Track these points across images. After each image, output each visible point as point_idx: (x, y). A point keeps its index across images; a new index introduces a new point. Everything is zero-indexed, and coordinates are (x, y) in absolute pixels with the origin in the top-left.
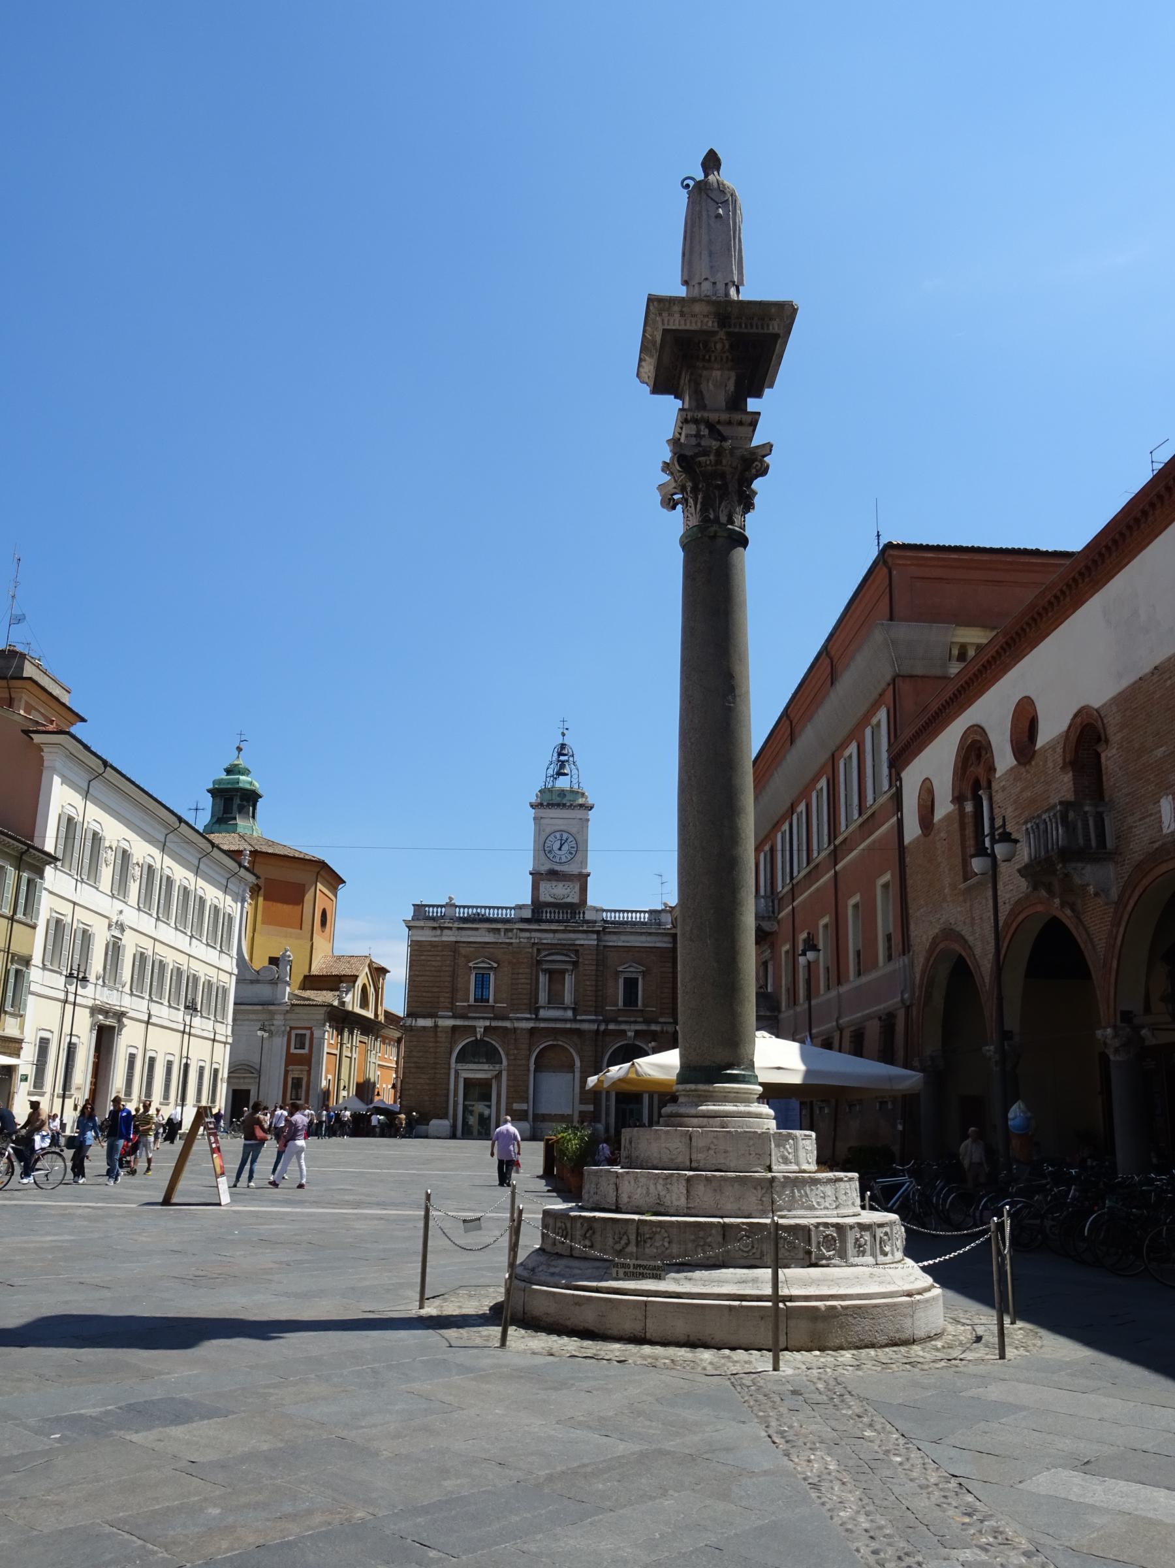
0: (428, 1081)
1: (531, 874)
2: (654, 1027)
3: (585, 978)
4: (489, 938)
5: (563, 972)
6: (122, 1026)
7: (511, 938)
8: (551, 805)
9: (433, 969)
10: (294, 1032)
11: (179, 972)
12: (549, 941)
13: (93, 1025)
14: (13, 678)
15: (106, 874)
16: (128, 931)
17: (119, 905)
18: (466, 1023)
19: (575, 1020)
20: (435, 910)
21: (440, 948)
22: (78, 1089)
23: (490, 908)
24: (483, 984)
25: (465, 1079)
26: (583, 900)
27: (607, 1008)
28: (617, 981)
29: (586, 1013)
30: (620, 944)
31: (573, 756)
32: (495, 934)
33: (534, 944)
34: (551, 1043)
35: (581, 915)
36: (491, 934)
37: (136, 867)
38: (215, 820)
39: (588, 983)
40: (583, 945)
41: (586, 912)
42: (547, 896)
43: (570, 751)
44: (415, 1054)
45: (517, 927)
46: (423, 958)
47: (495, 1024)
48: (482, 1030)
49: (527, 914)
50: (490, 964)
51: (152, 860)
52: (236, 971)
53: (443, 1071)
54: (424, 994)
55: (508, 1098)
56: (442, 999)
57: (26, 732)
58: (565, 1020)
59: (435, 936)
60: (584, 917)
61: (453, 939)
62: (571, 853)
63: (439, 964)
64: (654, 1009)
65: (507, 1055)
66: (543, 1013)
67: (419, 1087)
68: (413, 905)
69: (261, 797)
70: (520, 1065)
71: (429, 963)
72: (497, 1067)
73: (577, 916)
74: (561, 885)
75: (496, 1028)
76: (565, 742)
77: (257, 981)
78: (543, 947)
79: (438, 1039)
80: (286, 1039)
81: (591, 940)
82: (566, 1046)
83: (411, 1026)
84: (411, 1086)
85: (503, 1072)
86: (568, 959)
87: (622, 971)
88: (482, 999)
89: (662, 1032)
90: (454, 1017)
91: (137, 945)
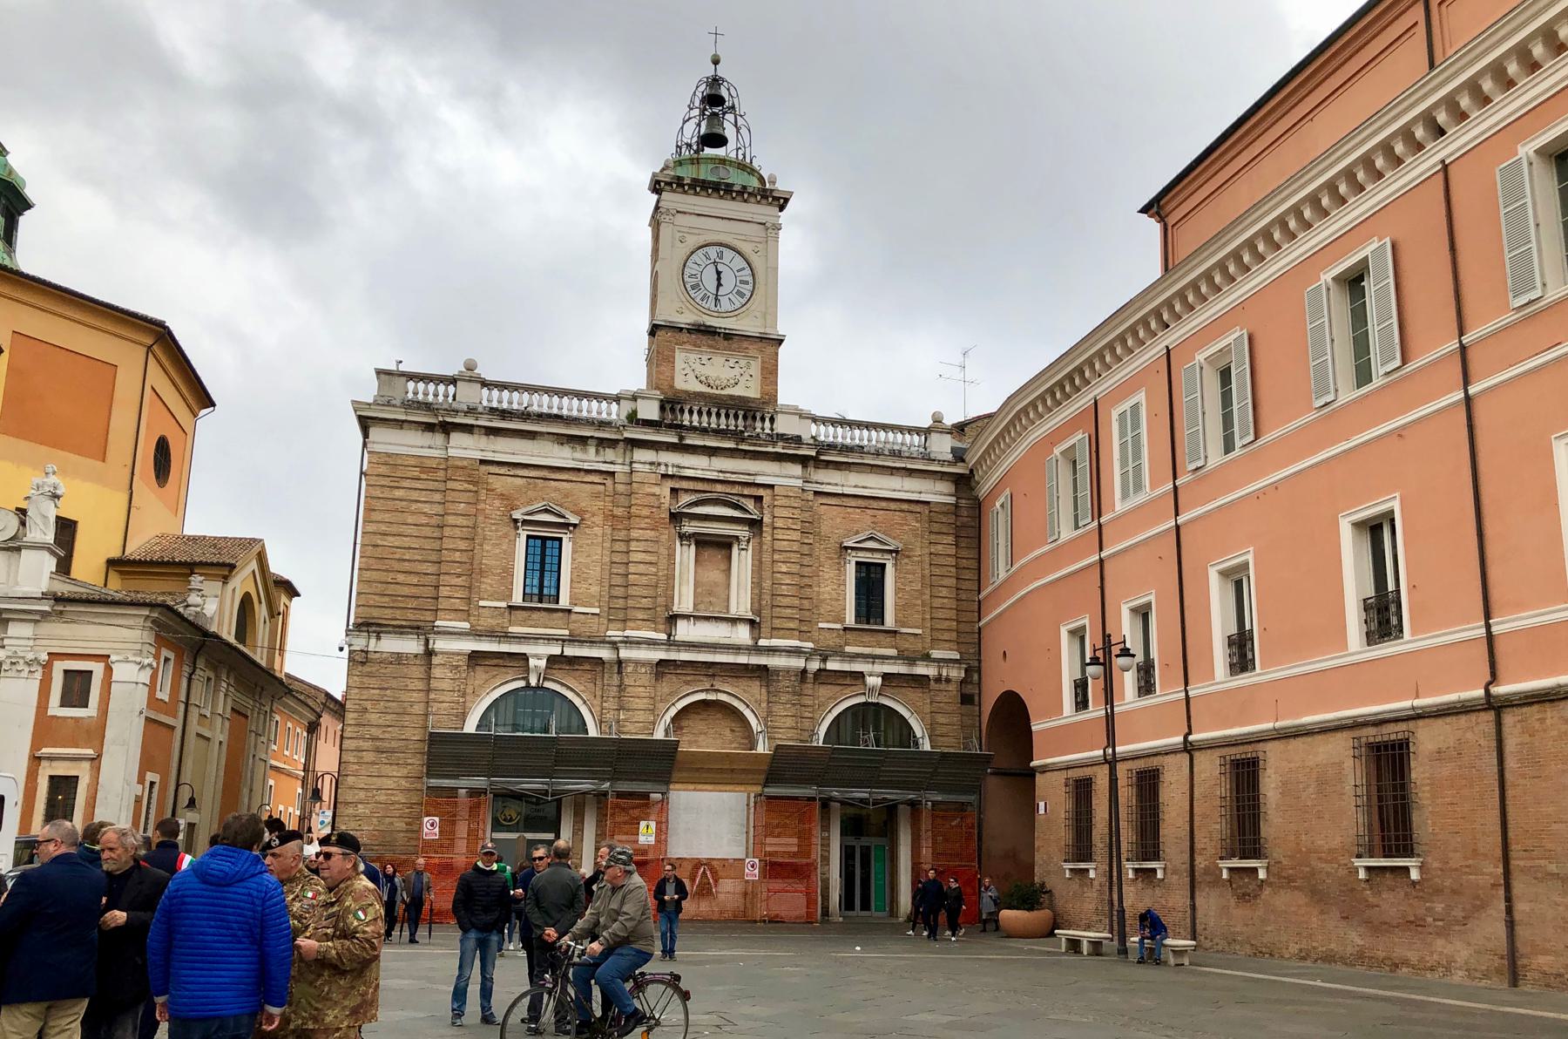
2: (921, 670)
3: (776, 557)
5: (724, 545)
7: (611, 463)
8: (701, 187)
9: (424, 520)
10: (59, 667)
12: (699, 474)
18: (505, 648)
19: (756, 649)
24: (543, 563)
26: (771, 398)
27: (821, 625)
28: (840, 568)
29: (775, 631)
30: (847, 491)
33: (664, 476)
34: (702, 696)
35: (767, 424)
39: (784, 568)
40: (772, 487)
41: (780, 419)
42: (691, 377)
44: (373, 718)
45: (627, 435)
46: (399, 493)
47: (570, 651)
48: (543, 663)
49: (649, 411)
54: (401, 578)
56: (444, 591)
58: (737, 649)
59: (430, 447)
60: (772, 429)
61: (479, 455)
63: (438, 509)
64: (920, 631)
66: (684, 631)
67: (383, 798)
68: (379, 372)
69: (27, 205)
71: (414, 507)
73: (758, 424)
74: (719, 360)
78: (685, 485)
81: (786, 477)
82: (736, 703)
84: (362, 795)
86: (737, 514)
87: (853, 548)
89: (938, 679)
90: (475, 634)
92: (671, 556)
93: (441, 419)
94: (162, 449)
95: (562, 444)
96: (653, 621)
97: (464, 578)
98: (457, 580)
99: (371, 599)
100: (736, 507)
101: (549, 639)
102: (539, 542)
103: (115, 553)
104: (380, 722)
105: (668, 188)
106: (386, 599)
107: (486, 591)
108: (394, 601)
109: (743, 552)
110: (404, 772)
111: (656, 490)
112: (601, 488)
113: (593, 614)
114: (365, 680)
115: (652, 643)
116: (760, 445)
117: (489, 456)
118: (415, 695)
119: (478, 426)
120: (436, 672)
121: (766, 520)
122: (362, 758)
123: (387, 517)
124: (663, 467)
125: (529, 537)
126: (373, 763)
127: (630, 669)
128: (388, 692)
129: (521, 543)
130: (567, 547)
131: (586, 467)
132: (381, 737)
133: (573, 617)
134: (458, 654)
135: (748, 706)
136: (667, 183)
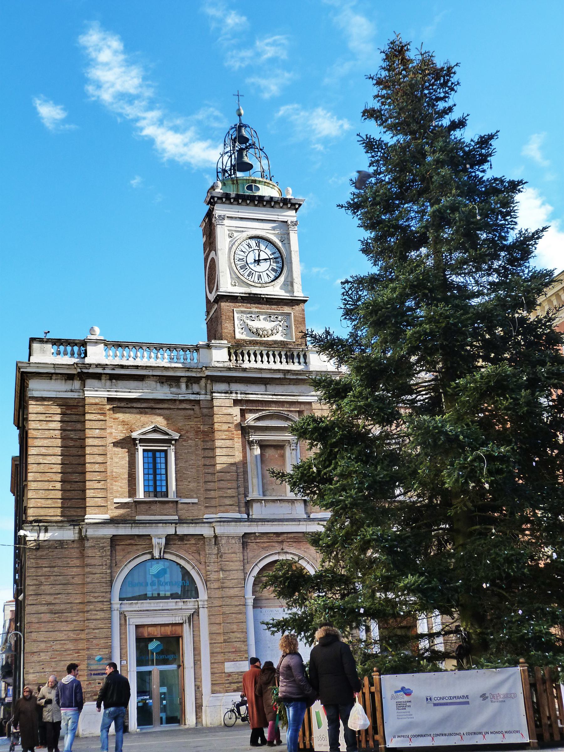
0: (72, 635)
7: (198, 394)
32: (171, 386)
33: (236, 402)
48: (163, 541)
50: (167, 434)
53: (101, 615)
55: (212, 654)
56: (89, 493)
59: (72, 391)
61: (106, 394)
65: (206, 582)
67: (58, 647)
70: (230, 597)
72: (191, 604)
73: (296, 360)
75: (183, 538)
76: (244, 122)
79: (88, 561)
85: (201, 610)
93: (79, 370)
95: (163, 383)
96: (239, 506)
97: (103, 482)
98: (98, 484)
99: (38, 502)
100: (287, 419)
102: (150, 454)
104: (52, 591)
105: (219, 201)
106: (49, 502)
107: (117, 492)
108: (54, 503)
109: (294, 452)
110: (71, 627)
111: (230, 411)
112: (192, 412)
113: (193, 503)
114: (39, 561)
116: (300, 374)
117: (113, 395)
118: (75, 570)
119: (104, 374)
120: (89, 552)
122: (41, 618)
123: (46, 442)
124: (234, 395)
125: (144, 451)
126: (49, 622)
127: (223, 542)
128: (56, 569)
131: (180, 398)
132: (53, 602)
133: (180, 506)
134: (103, 538)
135: (308, 563)
136: (219, 198)
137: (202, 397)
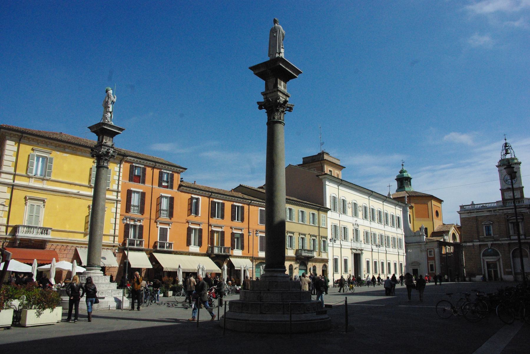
1: (500, 190)
4: (488, 214)
6: (362, 253)
7: (496, 213)
11: (381, 236)
13: (352, 253)
14: (321, 160)
15: (349, 211)
16: (360, 226)
17: (355, 219)
20: (469, 206)
21: (471, 219)
22: (350, 271)
23: (487, 203)
25: (487, 262)
31: (511, 146)
32: (490, 212)
33: (505, 214)
35: (522, 202)
36: (489, 212)
37: (360, 208)
38: (399, 188)
40: (525, 212)
43: (509, 145)
46: (466, 223)
48: (490, 245)
51: (365, 204)
52: (404, 234)
57: (317, 176)
61: (476, 216)
62: (515, 181)
65: (501, 253)
66: (512, 237)
68: (460, 206)
69: (412, 179)
72: (498, 257)
73: (521, 202)
76: (507, 142)
77: (415, 236)
80: (426, 253)
83: (465, 246)
88: (488, 234)
90: (479, 241)
91: (364, 230)
92: (508, 226)
94: (437, 212)
101: (490, 241)
103: (433, 231)
115: (506, 240)
117: (477, 215)
121: (524, 218)
129: (484, 228)
130: (491, 226)
137: (497, 214)
